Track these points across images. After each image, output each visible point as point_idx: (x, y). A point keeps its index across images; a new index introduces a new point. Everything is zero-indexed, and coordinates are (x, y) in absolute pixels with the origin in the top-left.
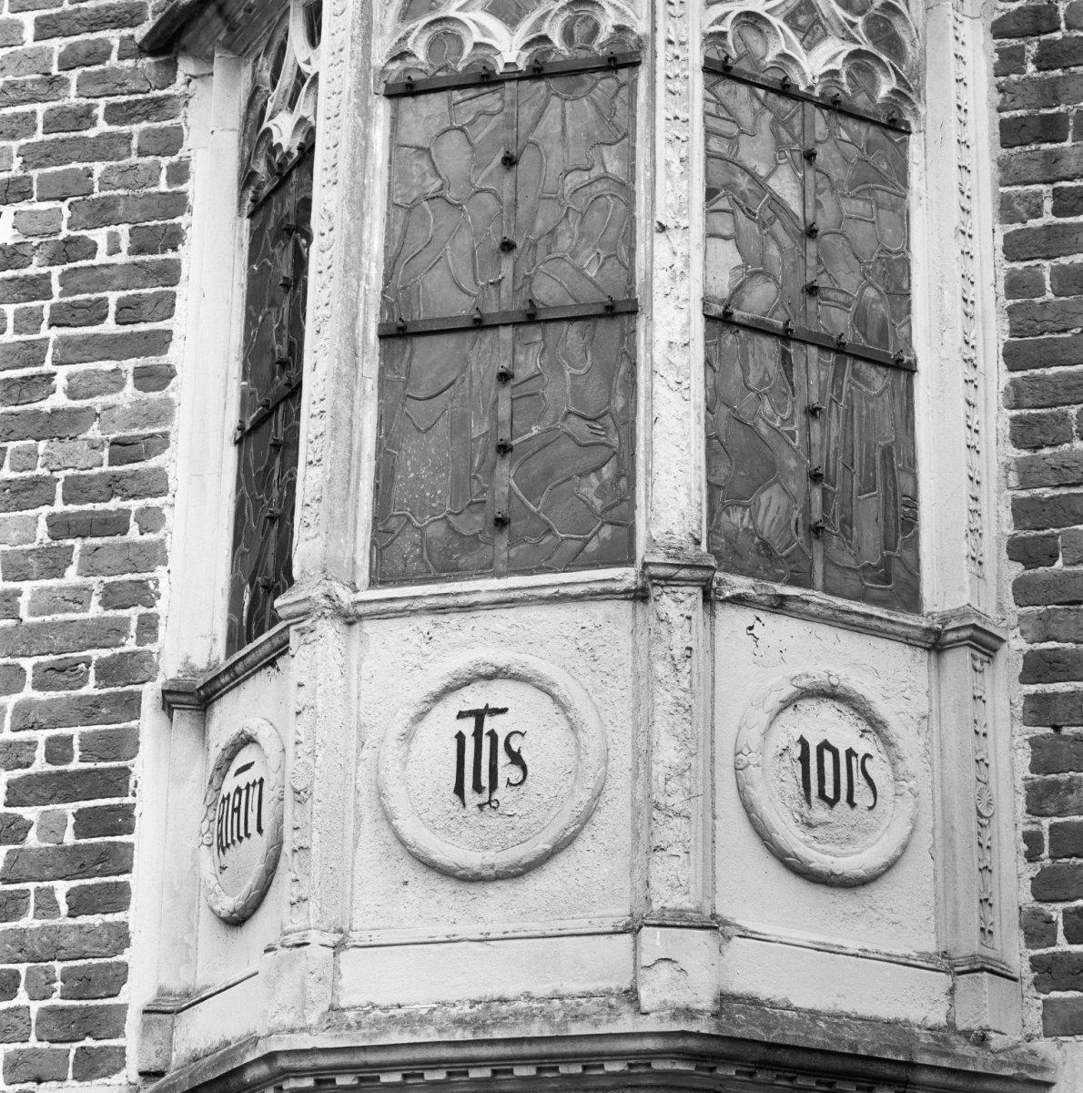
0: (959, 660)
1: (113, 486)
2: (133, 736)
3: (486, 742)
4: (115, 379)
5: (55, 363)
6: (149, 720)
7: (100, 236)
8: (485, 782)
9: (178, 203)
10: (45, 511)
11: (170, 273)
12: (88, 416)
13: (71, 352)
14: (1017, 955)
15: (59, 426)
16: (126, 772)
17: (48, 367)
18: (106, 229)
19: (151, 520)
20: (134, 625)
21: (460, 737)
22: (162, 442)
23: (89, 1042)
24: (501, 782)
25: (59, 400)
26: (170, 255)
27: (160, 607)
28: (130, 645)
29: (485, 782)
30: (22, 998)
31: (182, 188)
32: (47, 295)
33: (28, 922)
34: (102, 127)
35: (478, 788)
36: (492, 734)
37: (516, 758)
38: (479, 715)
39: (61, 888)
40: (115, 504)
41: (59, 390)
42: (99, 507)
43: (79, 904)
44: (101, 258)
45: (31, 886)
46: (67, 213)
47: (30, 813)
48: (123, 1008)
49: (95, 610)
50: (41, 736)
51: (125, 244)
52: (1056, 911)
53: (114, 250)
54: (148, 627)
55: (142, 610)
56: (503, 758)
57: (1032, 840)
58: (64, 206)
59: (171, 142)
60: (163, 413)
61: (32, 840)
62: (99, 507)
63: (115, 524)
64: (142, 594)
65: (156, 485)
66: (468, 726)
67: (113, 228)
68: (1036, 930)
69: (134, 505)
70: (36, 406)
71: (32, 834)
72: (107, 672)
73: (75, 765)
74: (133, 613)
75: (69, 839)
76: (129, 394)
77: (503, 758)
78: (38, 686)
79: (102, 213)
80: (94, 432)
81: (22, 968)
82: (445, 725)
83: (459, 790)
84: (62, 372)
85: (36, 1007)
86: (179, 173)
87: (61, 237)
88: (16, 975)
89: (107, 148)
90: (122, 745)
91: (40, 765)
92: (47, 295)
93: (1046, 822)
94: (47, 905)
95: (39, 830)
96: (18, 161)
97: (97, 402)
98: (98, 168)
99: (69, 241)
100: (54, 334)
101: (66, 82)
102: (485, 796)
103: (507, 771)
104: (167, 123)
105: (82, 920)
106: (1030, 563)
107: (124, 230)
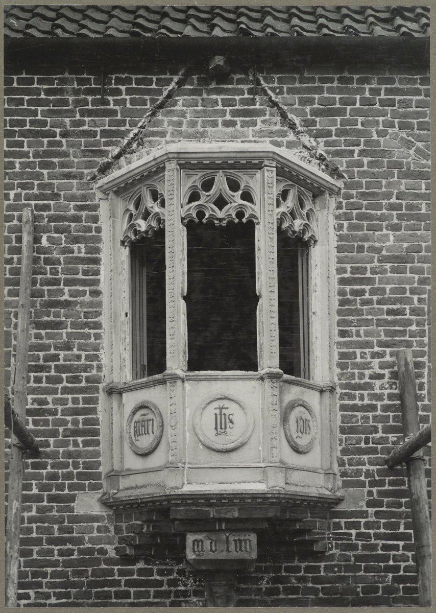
0: (327, 395)
1: (87, 325)
2: (97, 399)
3: (223, 416)
4: (83, 293)
5: (65, 285)
6: (102, 396)
7: (75, 247)
8: (223, 427)
9: (98, 240)
10: (65, 330)
11: (97, 261)
12: (76, 303)
13: (68, 283)
14: (336, 468)
15: (67, 304)
16: (96, 408)
17: (62, 286)
18: (77, 245)
19: (98, 337)
20: (95, 366)
21: (216, 414)
22: (98, 314)
23: (91, 481)
24: (228, 427)
25: (66, 297)
26: (98, 255)
27: (103, 362)
28: (94, 372)
29: (223, 427)
30: (71, 468)
31: (100, 234)
32: (60, 264)
33: (71, 448)
34: (72, 212)
35: (221, 428)
36: (225, 414)
37: (231, 422)
38: (221, 409)
39: (80, 439)
40: (87, 330)
41: (66, 294)
42: (82, 331)
43: (86, 444)
44: (76, 254)
45: (71, 439)
46: (64, 239)
47: (69, 418)
48: (101, 473)
49: (83, 362)
50: (70, 396)
51: (83, 250)
52: (346, 458)
53: (80, 252)
54: (99, 368)
55: (98, 363)
56: (228, 421)
57: (341, 440)
58: (63, 236)
59: (96, 219)
60: (100, 304)
61: (70, 426)
62: (82, 331)
63: (88, 336)
64: (96, 357)
65: (98, 326)
66: (218, 411)
67: (79, 245)
68: (342, 464)
69: (92, 331)
70: (59, 298)
71: (69, 424)
72: (88, 380)
73: (81, 405)
74: (95, 363)
75: (81, 426)
76: (87, 298)
77: (228, 421)
78: (67, 382)
79: (76, 240)
80: (78, 308)
81: (70, 461)
82: (212, 410)
83: (216, 429)
84: (67, 289)
85: (75, 471)
86: (98, 230)
87: (62, 246)
88: (69, 463)
89: (76, 219)
90: (95, 401)
91: (70, 405)
92: (60, 264)
93: (344, 436)
94: (76, 444)
95: (72, 423)
96: (46, 219)
97: (79, 299)
98: (73, 225)
99: (65, 247)
100: (64, 276)
101: (60, 196)
102: (223, 430)
103: (229, 425)
104: (94, 213)
105: (87, 448)
106: (342, 369)
107: (83, 246)
